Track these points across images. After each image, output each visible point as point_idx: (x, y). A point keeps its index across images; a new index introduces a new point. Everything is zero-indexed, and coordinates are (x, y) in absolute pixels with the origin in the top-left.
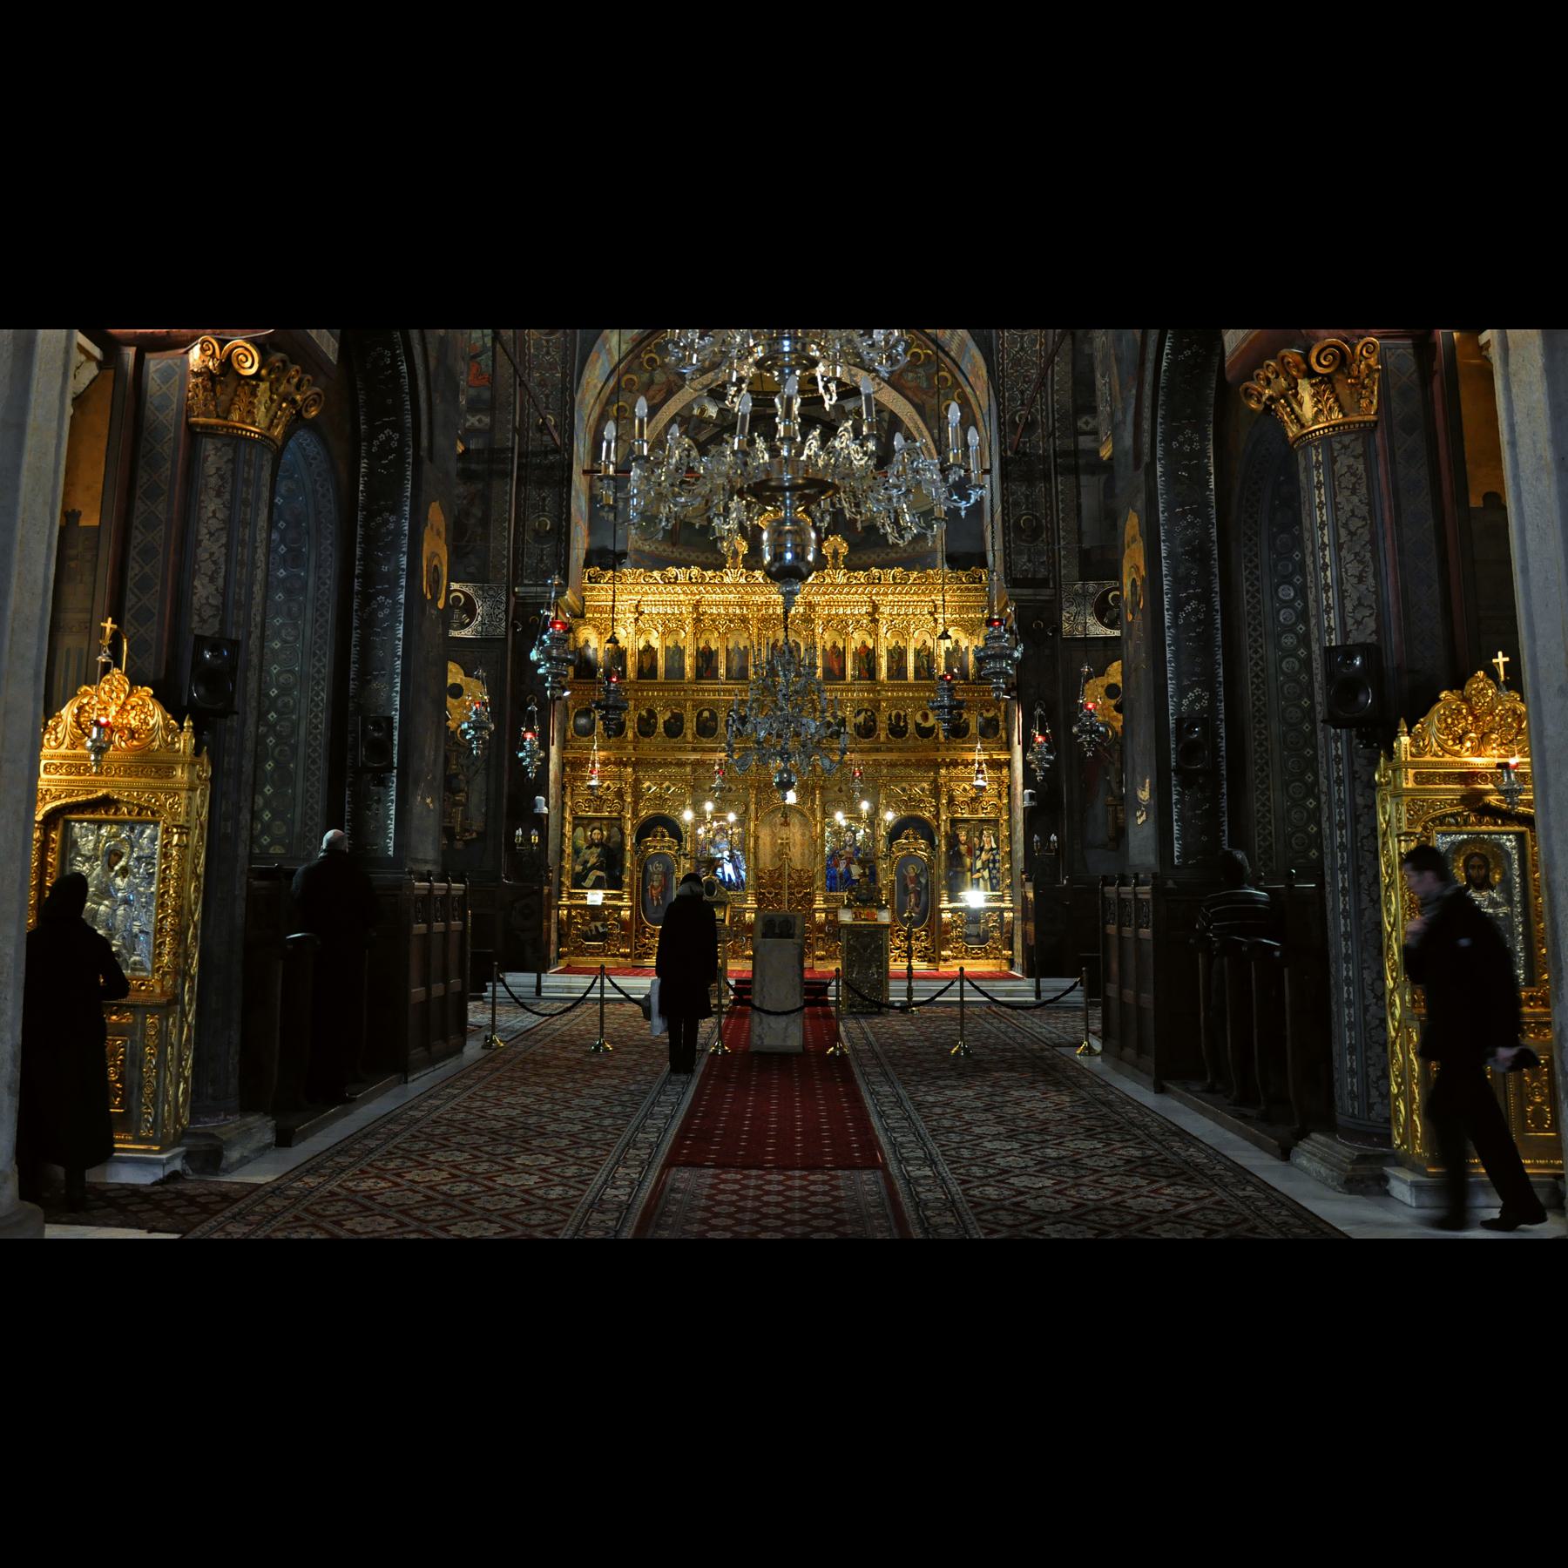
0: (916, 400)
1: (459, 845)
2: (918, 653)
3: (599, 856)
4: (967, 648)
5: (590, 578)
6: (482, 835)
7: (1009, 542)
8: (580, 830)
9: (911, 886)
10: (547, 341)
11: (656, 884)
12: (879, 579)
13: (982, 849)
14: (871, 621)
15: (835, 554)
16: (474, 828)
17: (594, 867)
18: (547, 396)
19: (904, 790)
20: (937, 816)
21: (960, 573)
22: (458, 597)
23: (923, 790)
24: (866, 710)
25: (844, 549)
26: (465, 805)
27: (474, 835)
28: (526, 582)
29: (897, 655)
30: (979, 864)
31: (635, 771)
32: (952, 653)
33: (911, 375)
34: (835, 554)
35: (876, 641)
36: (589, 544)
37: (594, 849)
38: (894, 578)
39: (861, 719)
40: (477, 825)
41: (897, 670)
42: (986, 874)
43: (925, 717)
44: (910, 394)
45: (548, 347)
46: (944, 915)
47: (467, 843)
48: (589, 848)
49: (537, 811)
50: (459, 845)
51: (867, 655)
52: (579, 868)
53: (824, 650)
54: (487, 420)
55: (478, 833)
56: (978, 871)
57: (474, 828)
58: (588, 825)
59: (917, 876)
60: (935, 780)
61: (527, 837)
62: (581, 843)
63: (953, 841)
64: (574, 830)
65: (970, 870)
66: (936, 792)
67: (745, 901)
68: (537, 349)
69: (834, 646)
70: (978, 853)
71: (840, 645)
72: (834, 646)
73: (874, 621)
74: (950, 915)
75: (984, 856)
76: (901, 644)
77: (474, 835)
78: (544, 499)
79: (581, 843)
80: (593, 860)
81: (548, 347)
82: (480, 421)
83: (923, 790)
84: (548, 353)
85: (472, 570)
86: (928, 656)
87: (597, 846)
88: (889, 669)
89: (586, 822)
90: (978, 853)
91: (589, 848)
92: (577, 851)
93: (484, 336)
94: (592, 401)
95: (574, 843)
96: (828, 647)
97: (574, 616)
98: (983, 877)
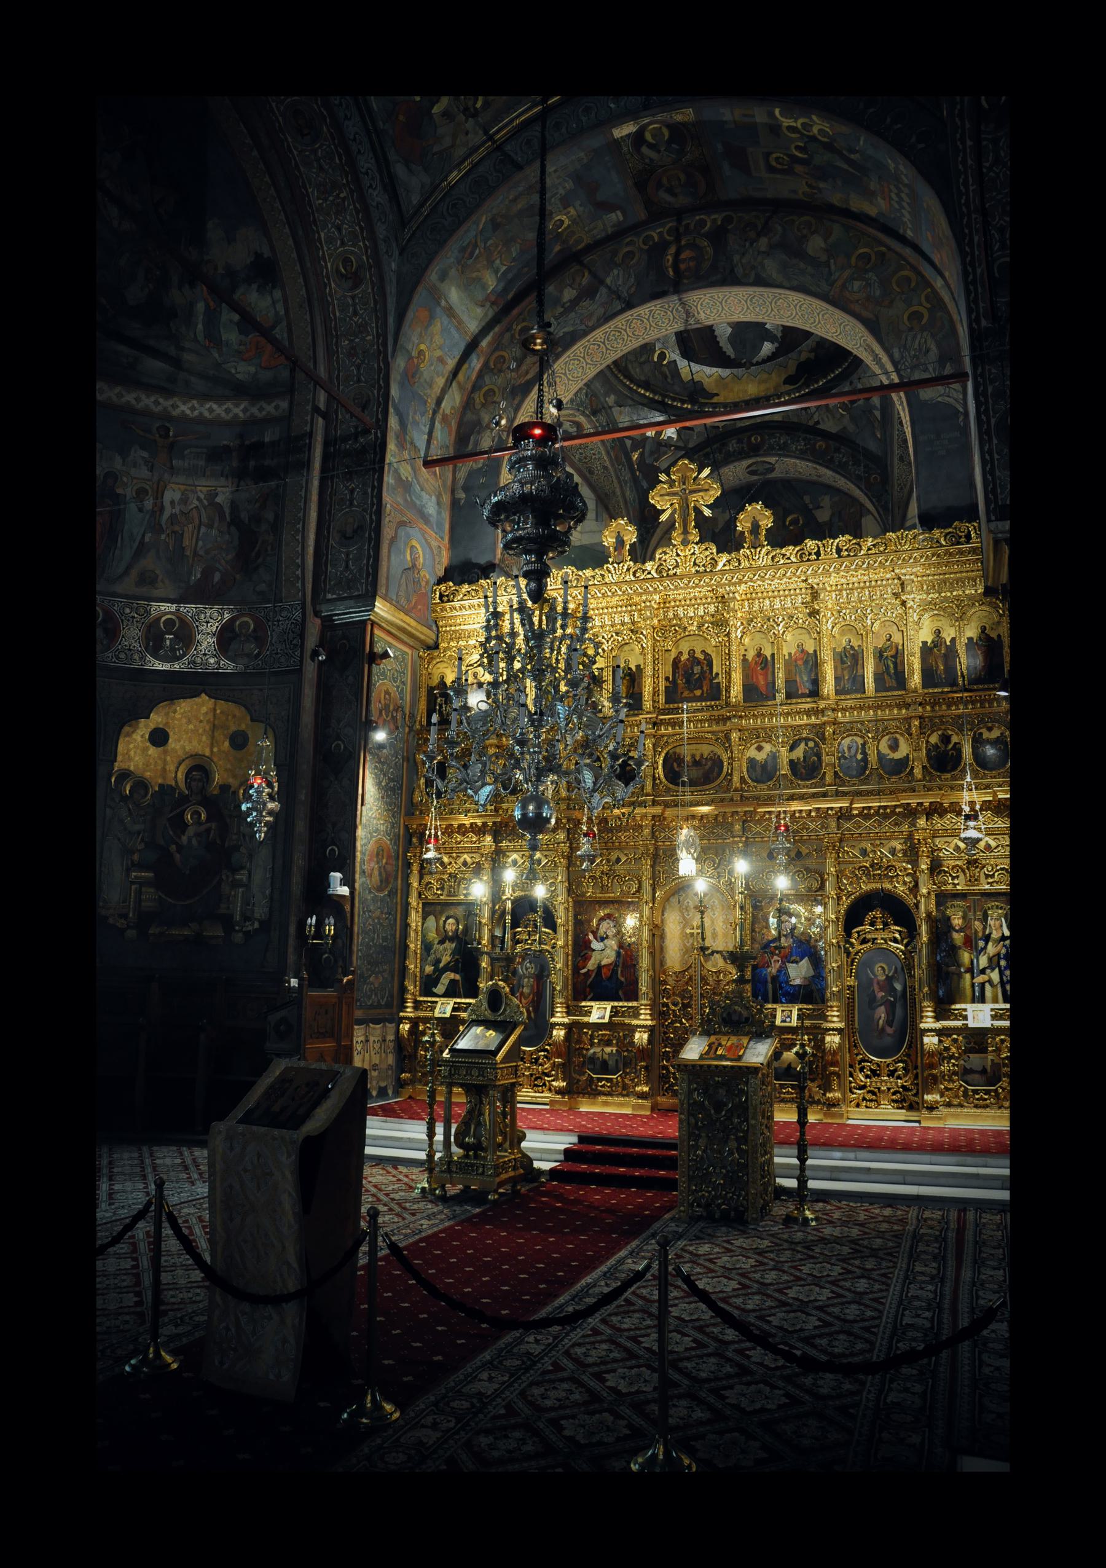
0: (866, 314)
1: (238, 938)
2: (880, 654)
3: (453, 953)
4: (953, 640)
5: (441, 596)
6: (265, 925)
7: (990, 452)
8: (431, 920)
9: (880, 994)
10: (353, 298)
11: (526, 990)
12: (818, 554)
13: (987, 938)
14: (810, 615)
15: (755, 528)
16: (257, 916)
17: (447, 968)
18: (358, 368)
19: (864, 852)
20: (915, 889)
21: (937, 533)
22: (247, 624)
23: (893, 852)
24: (807, 740)
25: (767, 521)
26: (247, 886)
27: (256, 925)
28: (329, 596)
29: (849, 659)
30: (983, 961)
31: (496, 840)
32: (931, 649)
33: (857, 285)
34: (755, 528)
35: (818, 641)
36: (451, 559)
37: (447, 945)
38: (839, 551)
39: (799, 753)
40: (260, 911)
41: (850, 683)
42: (995, 976)
43: (894, 747)
44: (857, 308)
45: (354, 305)
46: (926, 1040)
47: (247, 934)
48: (442, 942)
49: (331, 891)
50: (238, 938)
51: (806, 662)
52: (429, 969)
53: (744, 660)
54: (284, 405)
55: (261, 922)
56: (983, 972)
57: (257, 916)
58: (441, 913)
59: (889, 979)
60: (910, 836)
61: (320, 925)
62: (432, 935)
63: (941, 929)
64: (424, 919)
65: (970, 970)
66: (912, 853)
67: (636, 1015)
68: (341, 311)
69: (759, 654)
70: (981, 944)
71: (768, 653)
72: (759, 654)
73: (814, 613)
74: (935, 1040)
75: (991, 949)
76: (855, 643)
77: (256, 925)
78: (352, 491)
79: (432, 935)
80: (446, 959)
81: (354, 305)
82: (277, 408)
83: (893, 852)
84: (355, 313)
85: (262, 587)
86: (895, 656)
87: (451, 940)
88: (837, 679)
89: (439, 908)
90: (981, 944)
91: (442, 942)
92: (427, 947)
93: (274, 303)
94: (441, 382)
95: (424, 936)
96: (751, 655)
97: (429, 648)
98: (990, 981)
